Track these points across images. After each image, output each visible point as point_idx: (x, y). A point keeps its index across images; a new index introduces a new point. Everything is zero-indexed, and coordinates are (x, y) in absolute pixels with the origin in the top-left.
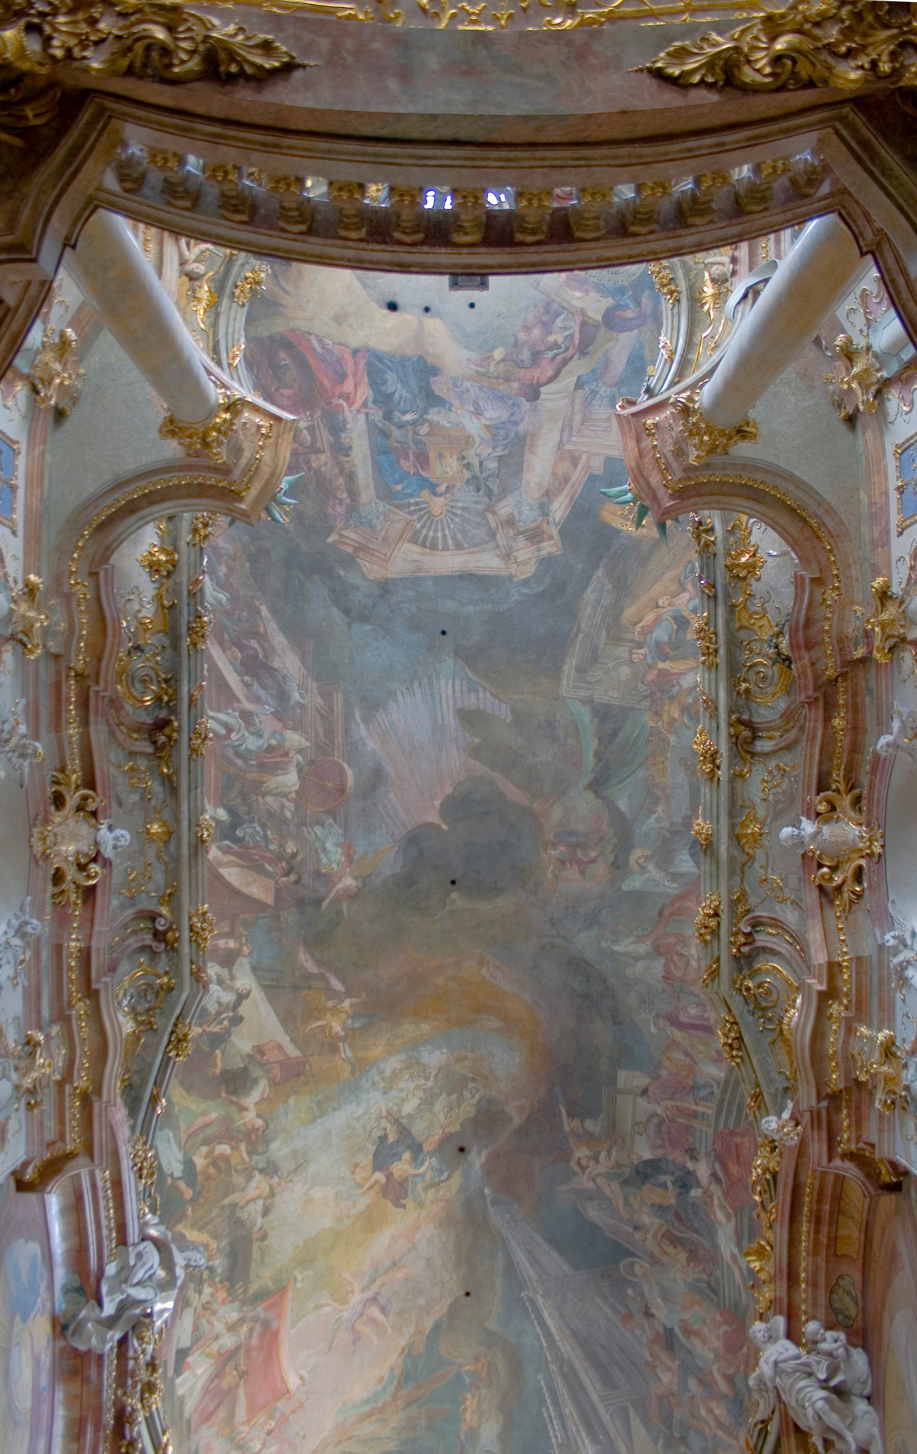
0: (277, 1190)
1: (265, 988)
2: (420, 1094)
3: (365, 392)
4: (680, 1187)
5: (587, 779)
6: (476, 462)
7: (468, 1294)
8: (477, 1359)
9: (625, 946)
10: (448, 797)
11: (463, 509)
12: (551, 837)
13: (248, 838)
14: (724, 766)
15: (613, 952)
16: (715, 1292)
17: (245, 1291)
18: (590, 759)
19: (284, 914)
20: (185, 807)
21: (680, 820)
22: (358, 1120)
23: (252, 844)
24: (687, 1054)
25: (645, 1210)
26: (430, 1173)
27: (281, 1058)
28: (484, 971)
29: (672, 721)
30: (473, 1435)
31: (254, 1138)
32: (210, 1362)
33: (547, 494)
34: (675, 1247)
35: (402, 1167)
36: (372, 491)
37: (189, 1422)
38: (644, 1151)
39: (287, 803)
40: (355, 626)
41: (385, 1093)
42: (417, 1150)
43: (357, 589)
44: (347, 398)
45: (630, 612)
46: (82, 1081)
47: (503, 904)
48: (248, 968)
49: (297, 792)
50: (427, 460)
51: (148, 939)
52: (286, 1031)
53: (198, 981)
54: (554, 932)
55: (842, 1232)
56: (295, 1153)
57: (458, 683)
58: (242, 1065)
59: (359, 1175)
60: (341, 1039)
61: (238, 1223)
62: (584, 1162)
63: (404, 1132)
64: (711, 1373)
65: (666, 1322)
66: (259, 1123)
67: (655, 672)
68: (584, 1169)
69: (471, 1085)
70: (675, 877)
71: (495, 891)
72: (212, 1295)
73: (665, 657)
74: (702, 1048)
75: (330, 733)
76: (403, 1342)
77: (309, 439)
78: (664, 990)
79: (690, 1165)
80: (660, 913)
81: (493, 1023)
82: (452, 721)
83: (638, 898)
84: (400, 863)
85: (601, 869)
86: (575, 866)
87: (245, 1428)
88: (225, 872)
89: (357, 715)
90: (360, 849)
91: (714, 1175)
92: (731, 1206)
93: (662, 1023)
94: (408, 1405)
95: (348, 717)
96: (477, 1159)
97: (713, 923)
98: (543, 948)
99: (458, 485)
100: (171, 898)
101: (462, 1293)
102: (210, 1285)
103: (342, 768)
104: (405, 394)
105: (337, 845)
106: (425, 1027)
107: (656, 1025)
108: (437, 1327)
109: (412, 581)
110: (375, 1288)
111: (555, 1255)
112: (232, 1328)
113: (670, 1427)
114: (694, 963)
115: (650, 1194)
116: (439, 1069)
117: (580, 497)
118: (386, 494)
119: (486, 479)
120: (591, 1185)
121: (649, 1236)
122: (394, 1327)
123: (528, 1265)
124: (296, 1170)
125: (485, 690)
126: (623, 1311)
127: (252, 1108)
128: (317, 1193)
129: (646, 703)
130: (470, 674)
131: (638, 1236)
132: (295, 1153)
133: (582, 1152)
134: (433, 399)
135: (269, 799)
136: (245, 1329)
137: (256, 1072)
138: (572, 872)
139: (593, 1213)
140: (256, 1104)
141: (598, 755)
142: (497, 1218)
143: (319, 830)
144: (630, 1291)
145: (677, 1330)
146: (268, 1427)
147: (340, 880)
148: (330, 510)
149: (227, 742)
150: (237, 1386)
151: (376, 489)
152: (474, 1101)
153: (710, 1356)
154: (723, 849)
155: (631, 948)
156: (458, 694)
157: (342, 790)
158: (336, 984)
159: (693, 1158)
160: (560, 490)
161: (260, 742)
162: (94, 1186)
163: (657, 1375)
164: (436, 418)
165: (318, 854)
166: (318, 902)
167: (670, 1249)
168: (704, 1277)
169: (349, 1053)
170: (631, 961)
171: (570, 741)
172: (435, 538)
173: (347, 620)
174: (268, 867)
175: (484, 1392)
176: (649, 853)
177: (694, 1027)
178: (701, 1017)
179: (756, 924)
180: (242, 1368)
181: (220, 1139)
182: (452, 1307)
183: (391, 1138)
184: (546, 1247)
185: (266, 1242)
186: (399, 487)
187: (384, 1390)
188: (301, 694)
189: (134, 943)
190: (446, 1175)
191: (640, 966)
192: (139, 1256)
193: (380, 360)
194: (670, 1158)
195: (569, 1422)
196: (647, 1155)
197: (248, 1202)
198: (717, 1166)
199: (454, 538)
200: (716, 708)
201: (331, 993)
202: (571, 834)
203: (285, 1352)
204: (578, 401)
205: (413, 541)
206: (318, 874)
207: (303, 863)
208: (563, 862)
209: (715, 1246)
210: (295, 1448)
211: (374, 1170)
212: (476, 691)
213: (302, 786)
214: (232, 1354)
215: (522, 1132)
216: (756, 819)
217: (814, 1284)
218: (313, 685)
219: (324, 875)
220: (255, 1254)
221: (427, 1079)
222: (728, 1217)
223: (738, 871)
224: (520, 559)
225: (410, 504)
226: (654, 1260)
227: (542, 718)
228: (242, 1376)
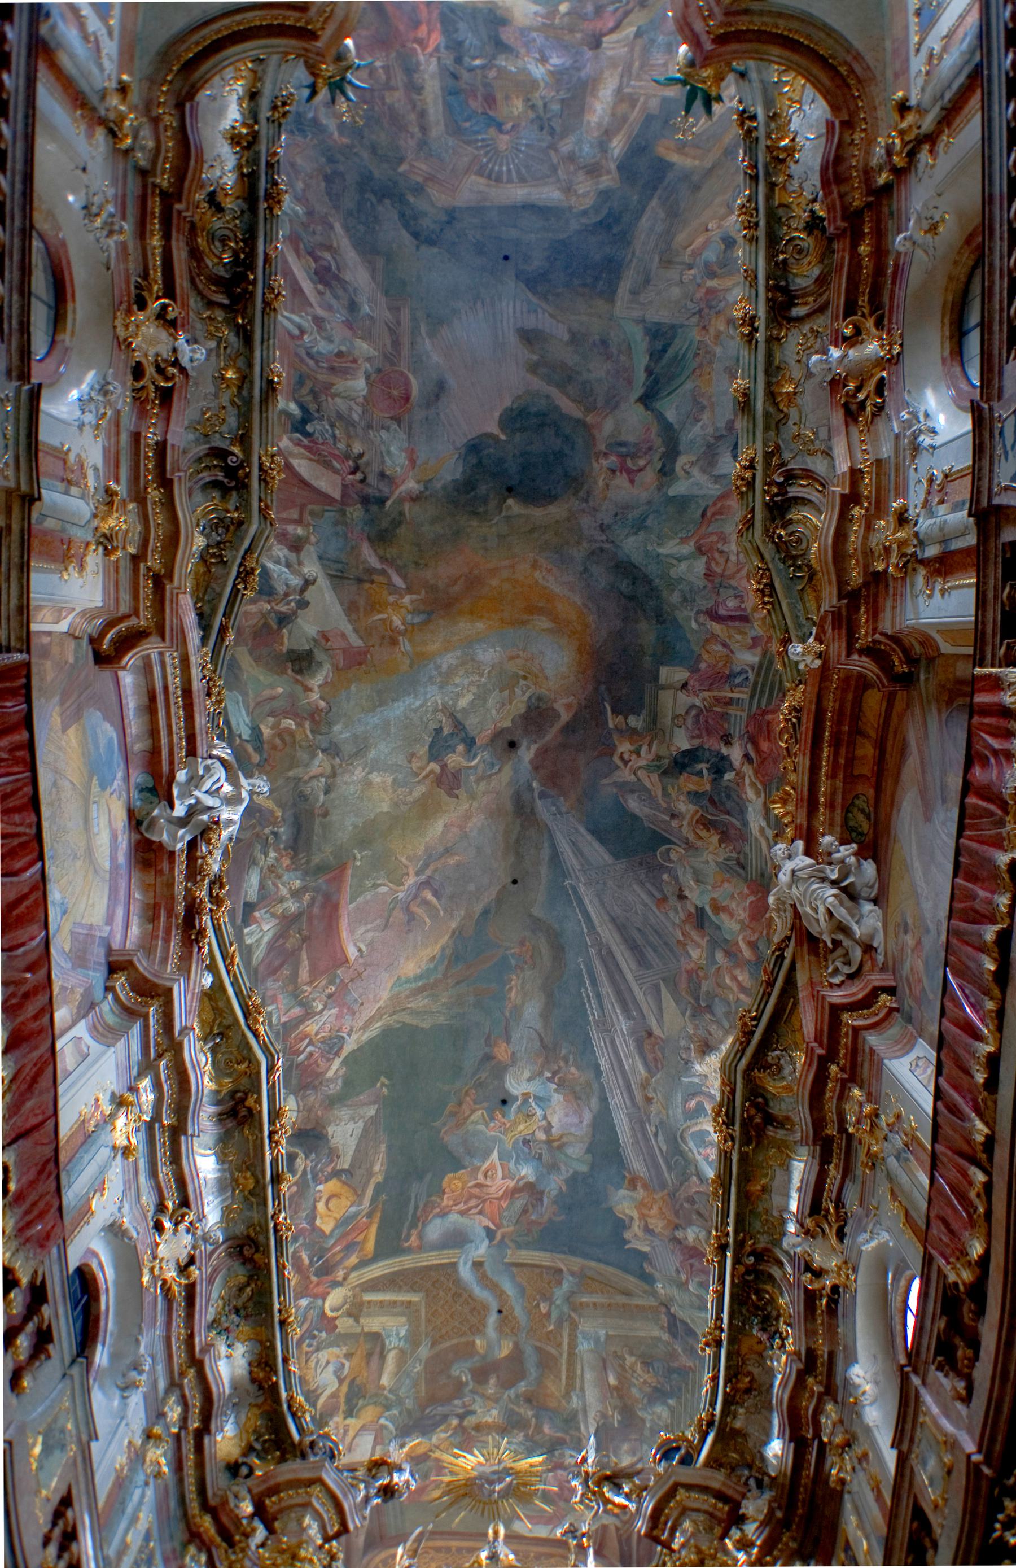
0: (339, 771)
1: (331, 577)
2: (474, 689)
3: (436, 39)
4: (716, 773)
5: (638, 391)
6: (540, 103)
7: (515, 882)
8: (522, 943)
9: (670, 548)
10: (506, 410)
11: (527, 146)
12: (602, 447)
13: (317, 435)
14: (762, 328)
15: (658, 555)
16: (743, 867)
17: (308, 862)
18: (641, 376)
19: (349, 510)
20: (257, 354)
21: (723, 425)
22: (415, 711)
23: (321, 441)
24: (725, 645)
25: (682, 798)
26: (482, 765)
27: (344, 645)
28: (537, 575)
29: (718, 335)
30: (517, 1012)
31: (317, 718)
32: (274, 922)
33: (607, 132)
34: (708, 830)
35: (455, 759)
36: (442, 127)
37: (256, 971)
38: (683, 742)
39: (355, 407)
40: (423, 248)
41: (441, 687)
42: (470, 743)
45: (681, 238)
46: (154, 561)
47: (556, 511)
48: (315, 556)
49: (364, 397)
51: (220, 476)
52: (349, 621)
53: (265, 518)
54: (604, 538)
55: (859, 752)
56: (355, 737)
58: (307, 648)
59: (415, 766)
60: (400, 633)
61: (303, 797)
62: (626, 756)
63: (458, 726)
64: (737, 943)
65: (698, 903)
66: (322, 704)
67: (704, 290)
68: (626, 763)
69: (522, 682)
70: (718, 479)
71: (549, 498)
72: (277, 860)
73: (712, 275)
74: (739, 637)
75: (396, 344)
76: (454, 925)
78: (705, 587)
79: (725, 751)
80: (703, 515)
81: (544, 623)
82: (513, 339)
83: (682, 503)
84: (460, 469)
85: (649, 477)
86: (625, 474)
87: (305, 988)
88: (295, 463)
89: (423, 329)
90: (422, 456)
91: (747, 756)
92: (762, 782)
93: (702, 618)
94: (458, 983)
95: (415, 331)
96: (527, 753)
97: (748, 475)
98: (593, 553)
99: (523, 124)
100: (244, 439)
101: (510, 880)
102: (275, 851)
103: (407, 379)
105: (401, 450)
106: (480, 626)
107: (696, 621)
108: (486, 912)
109: (477, 210)
110: (428, 872)
111: (597, 845)
112: (296, 894)
113: (697, 999)
114: (733, 558)
115: (687, 782)
116: (493, 667)
117: (637, 135)
119: (549, 119)
120: (632, 778)
121: (685, 823)
122: (445, 910)
123: (571, 855)
124: (356, 754)
125: (544, 311)
126: (658, 895)
127: (316, 689)
128: (376, 778)
129: (695, 320)
130: (530, 295)
131: (675, 823)
132: (355, 737)
133: (624, 747)
135: (338, 400)
136: (307, 897)
137: (319, 655)
138: (621, 480)
139: (633, 804)
140: (320, 686)
141: (649, 371)
142: (543, 809)
143: (384, 434)
144: (665, 877)
145: (708, 909)
146: (328, 991)
147: (403, 482)
148: (402, 142)
149: (299, 343)
150: (300, 949)
151: (446, 125)
152: (525, 698)
153: (737, 927)
154: (760, 406)
155: (675, 550)
156: (518, 314)
157: (407, 399)
158: (397, 581)
159: (728, 743)
160: (619, 130)
161: (331, 347)
162: (166, 688)
163: (688, 952)
165: (382, 456)
166: (382, 501)
167: (703, 833)
168: (734, 855)
169: (408, 647)
170: (675, 562)
171: (623, 358)
172: (500, 172)
173: (415, 242)
174: (335, 463)
175: (528, 973)
176: (694, 459)
177: (732, 618)
178: (739, 608)
179: (791, 476)
180: (305, 933)
181: (286, 714)
182: (499, 893)
183: (446, 731)
184: (589, 837)
185: (328, 819)
186: (468, 125)
187: (436, 967)
189: (207, 476)
190: (497, 768)
191: (683, 566)
192: (207, 769)
193: (452, 11)
194: (706, 746)
195: (605, 1001)
196: (685, 746)
197: (311, 778)
198: (749, 746)
199: (518, 172)
200: (756, 277)
201: (393, 589)
202: (621, 444)
203: (344, 924)
204: (637, 49)
205: (480, 173)
206: (382, 475)
207: (368, 464)
208: (613, 471)
209: (745, 823)
210: (354, 1014)
211: (429, 761)
212: (535, 311)
213: (370, 392)
214: (296, 917)
215: (569, 729)
216: (791, 380)
217: (831, 806)
218: (381, 299)
219: (388, 477)
220: (317, 829)
221: (481, 675)
222: (758, 793)
223: (773, 426)
224: (581, 192)
225: (477, 141)
226: (689, 845)
227: (597, 337)
228: (304, 939)
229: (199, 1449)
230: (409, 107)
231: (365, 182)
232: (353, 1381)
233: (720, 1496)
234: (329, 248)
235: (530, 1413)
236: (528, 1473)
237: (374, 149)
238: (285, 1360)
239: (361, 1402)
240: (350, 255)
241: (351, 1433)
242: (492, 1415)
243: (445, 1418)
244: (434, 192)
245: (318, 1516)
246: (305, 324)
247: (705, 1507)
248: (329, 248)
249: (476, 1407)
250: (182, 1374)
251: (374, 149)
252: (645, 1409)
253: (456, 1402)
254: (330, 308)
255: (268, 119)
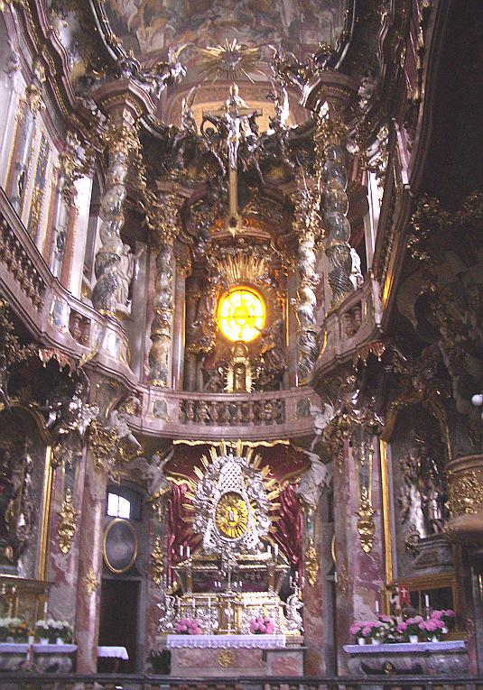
229: (60, 84)
232: (146, 6)
233: (345, 88)
235: (252, 15)
236: (249, 56)
238: (100, 18)
239: (153, 17)
241: (150, 36)
242: (232, 17)
243: (204, 19)
245: (130, 109)
247: (337, 95)
249: (221, 13)
250: (40, 49)
252: (318, 12)
253: (209, 11)
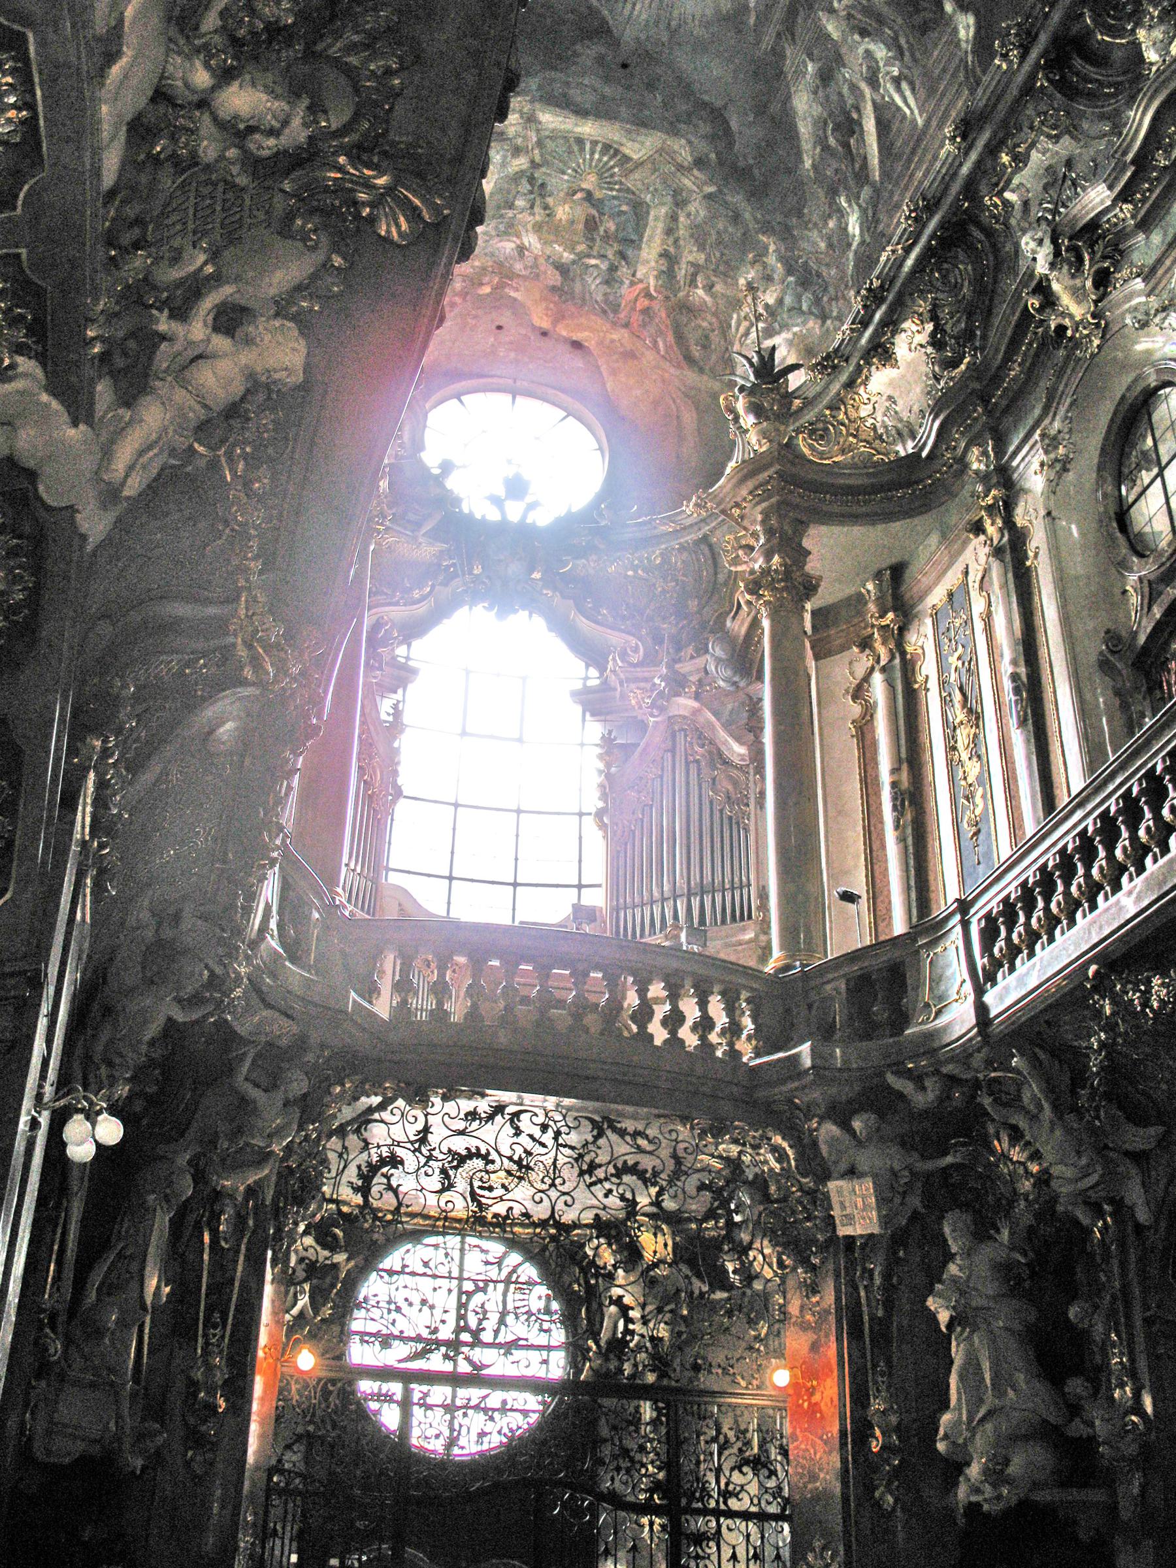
11: (564, 173)
20: (965, 170)
40: (719, 103)
43: (705, 137)
44: (648, 295)
50: (587, 222)
57: (626, 12)
77: (699, 279)
99: (562, 194)
100: (1028, 89)
104: (590, 280)
109: (642, 123)
118: (639, 210)
130: (609, 18)
134: (563, 269)
148: (702, 213)
151: (648, 213)
161: (872, 47)
164: (566, 254)
172: (603, 153)
186: (624, 208)
188: (806, 67)
199: (582, 150)
205: (627, 159)
225: (618, 191)
230: (682, 242)
231: (757, 193)
234: (826, 148)
237: (736, 218)
240: (805, 129)
244: (685, 155)
246: (890, 87)
248: (826, 148)
251: (736, 218)
254: (854, 88)
255: (847, 360)
